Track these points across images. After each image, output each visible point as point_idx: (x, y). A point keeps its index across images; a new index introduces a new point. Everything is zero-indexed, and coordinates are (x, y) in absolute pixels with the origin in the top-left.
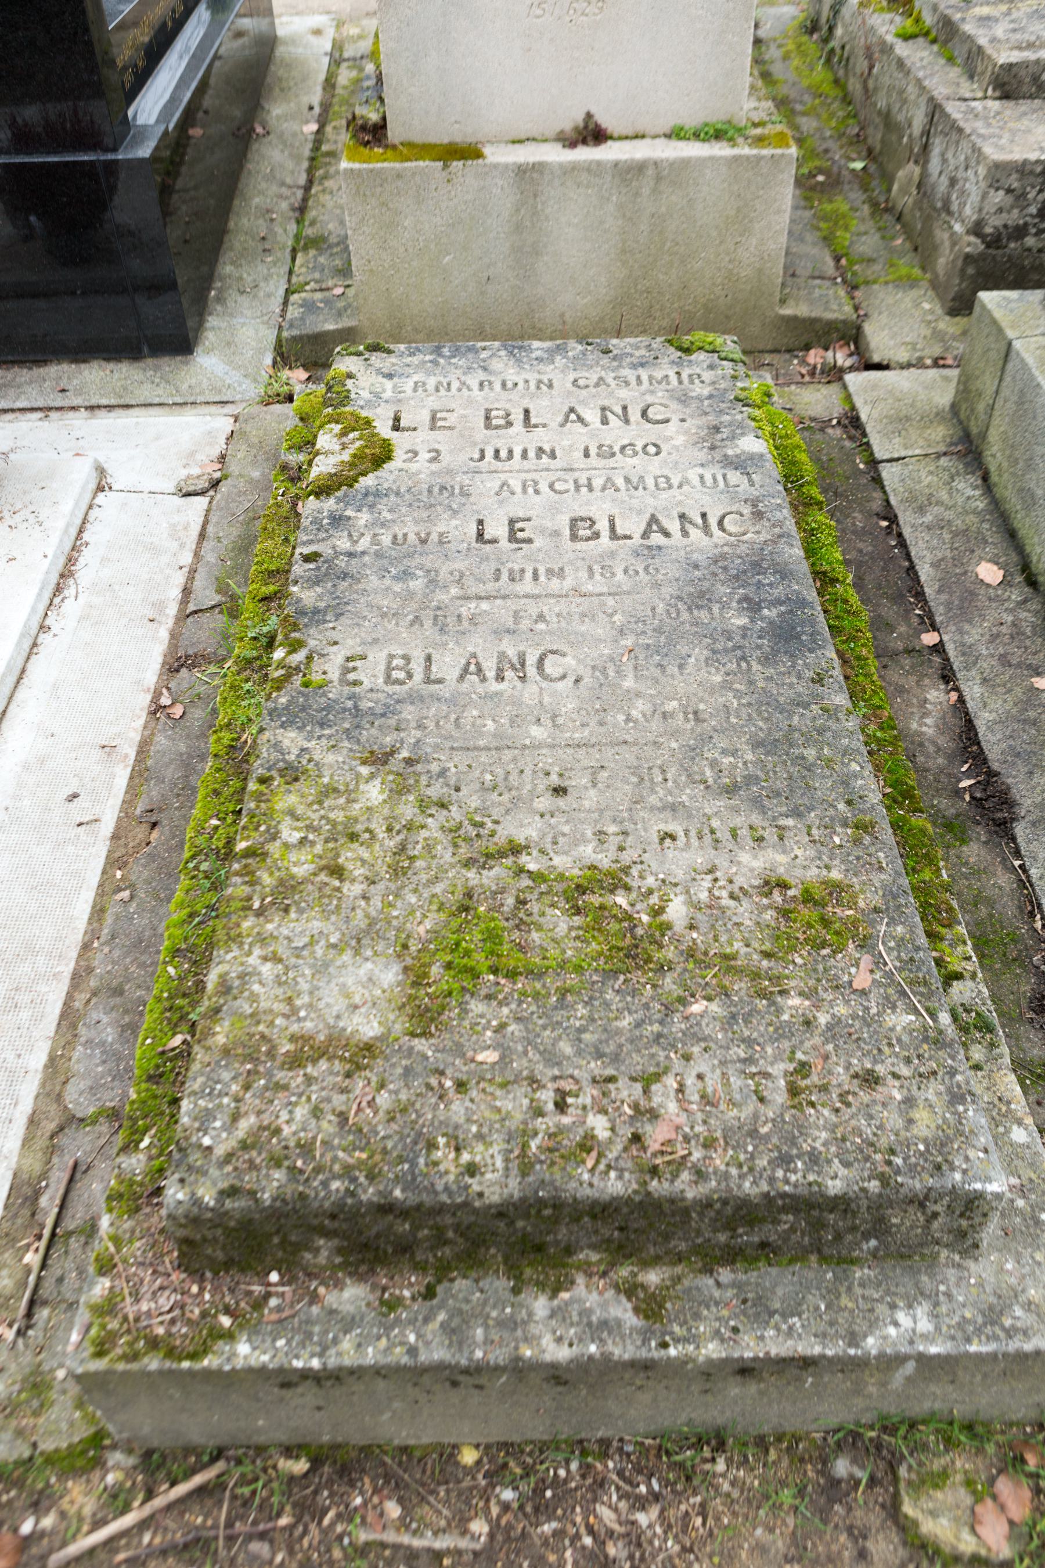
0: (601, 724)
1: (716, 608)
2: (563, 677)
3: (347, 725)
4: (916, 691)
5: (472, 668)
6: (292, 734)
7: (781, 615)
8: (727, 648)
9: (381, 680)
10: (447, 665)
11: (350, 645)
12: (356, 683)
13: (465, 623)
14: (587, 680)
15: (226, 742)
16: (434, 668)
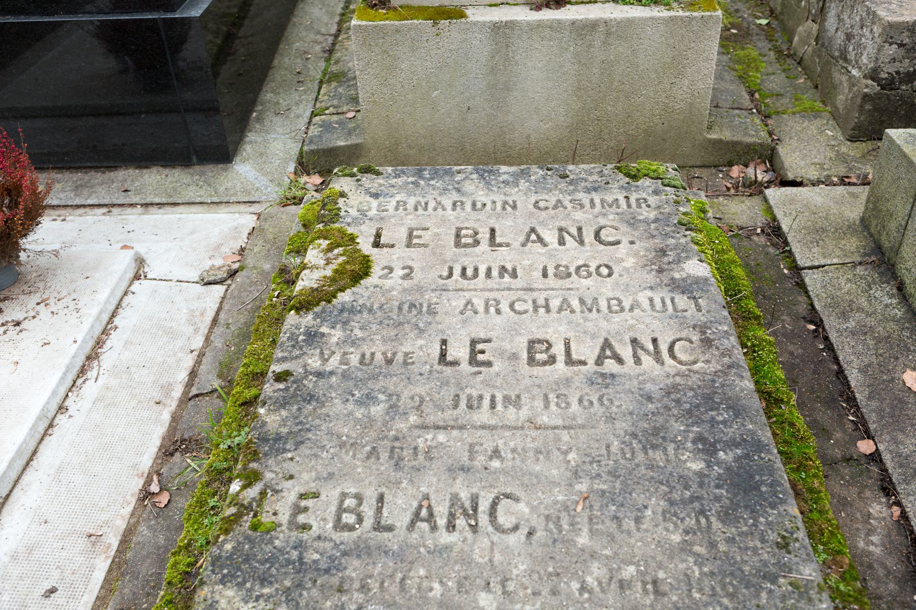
0: (554, 592)
1: (671, 448)
2: (516, 528)
3: (288, 583)
4: (859, 504)
5: (424, 513)
6: (230, 593)
7: (737, 459)
8: (684, 499)
9: (330, 525)
10: (399, 511)
11: (305, 481)
12: (306, 527)
13: (421, 457)
14: (540, 534)
15: (182, 568)
16: (385, 514)
